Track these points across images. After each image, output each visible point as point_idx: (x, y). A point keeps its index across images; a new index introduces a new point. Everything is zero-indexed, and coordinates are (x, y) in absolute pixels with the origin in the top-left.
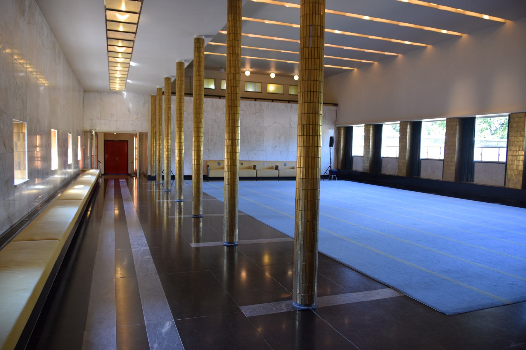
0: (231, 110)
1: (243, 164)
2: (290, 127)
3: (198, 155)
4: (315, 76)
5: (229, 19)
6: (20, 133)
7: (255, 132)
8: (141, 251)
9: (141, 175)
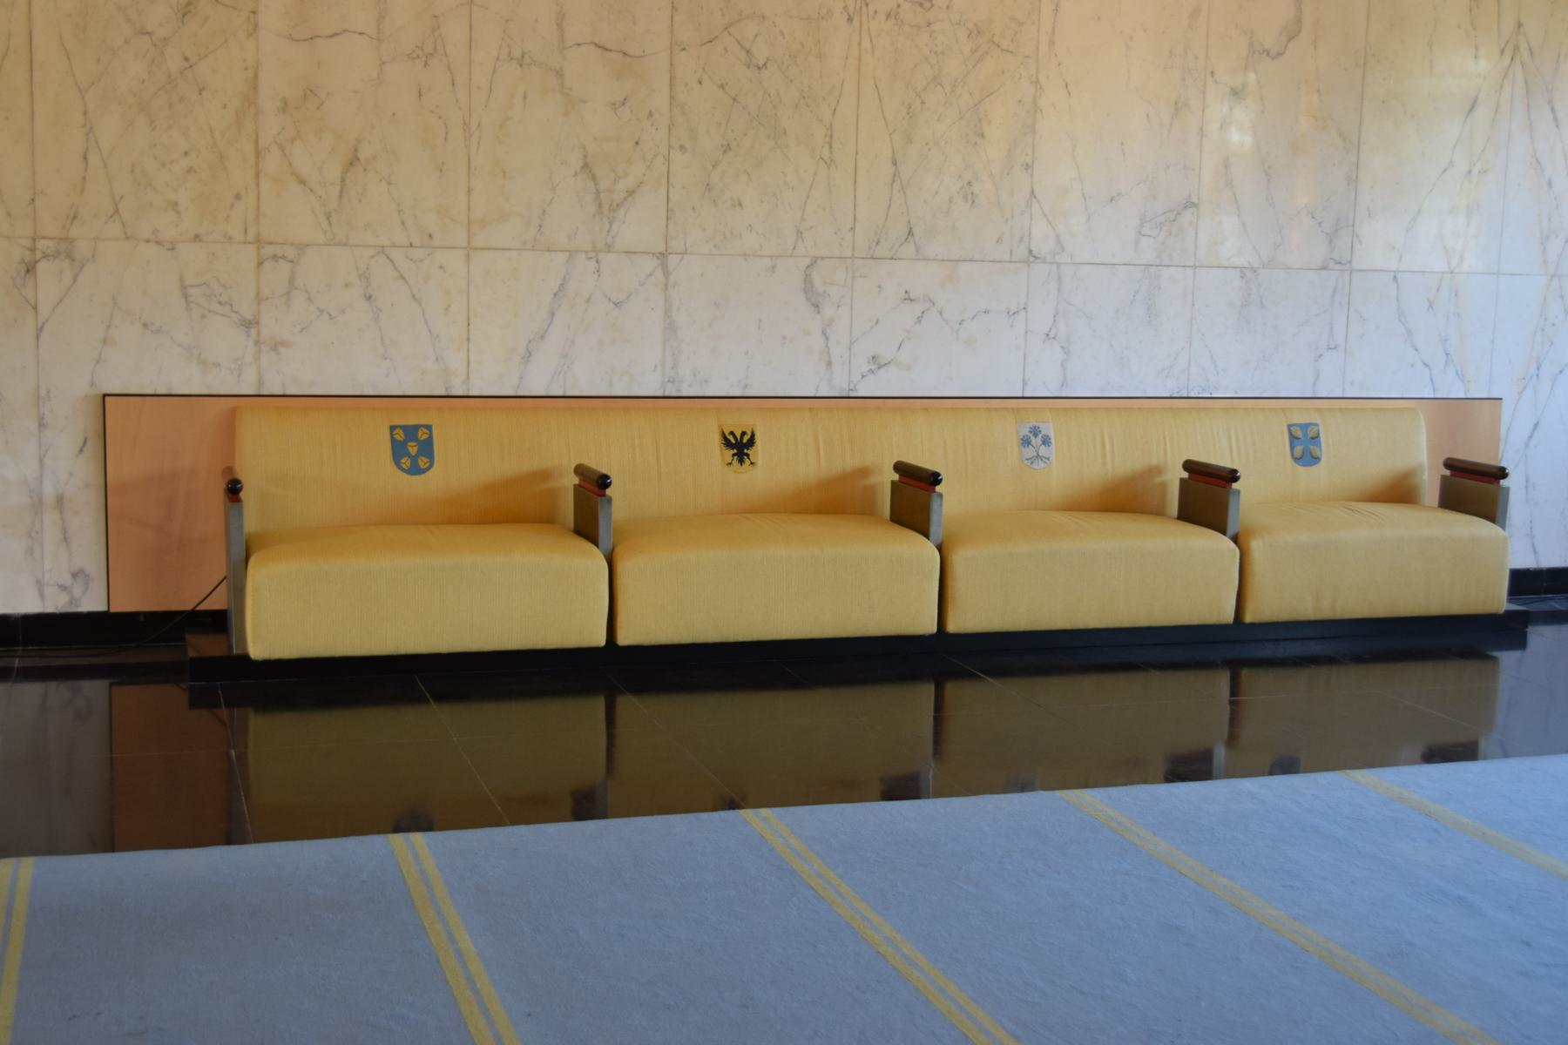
1: (758, 452)
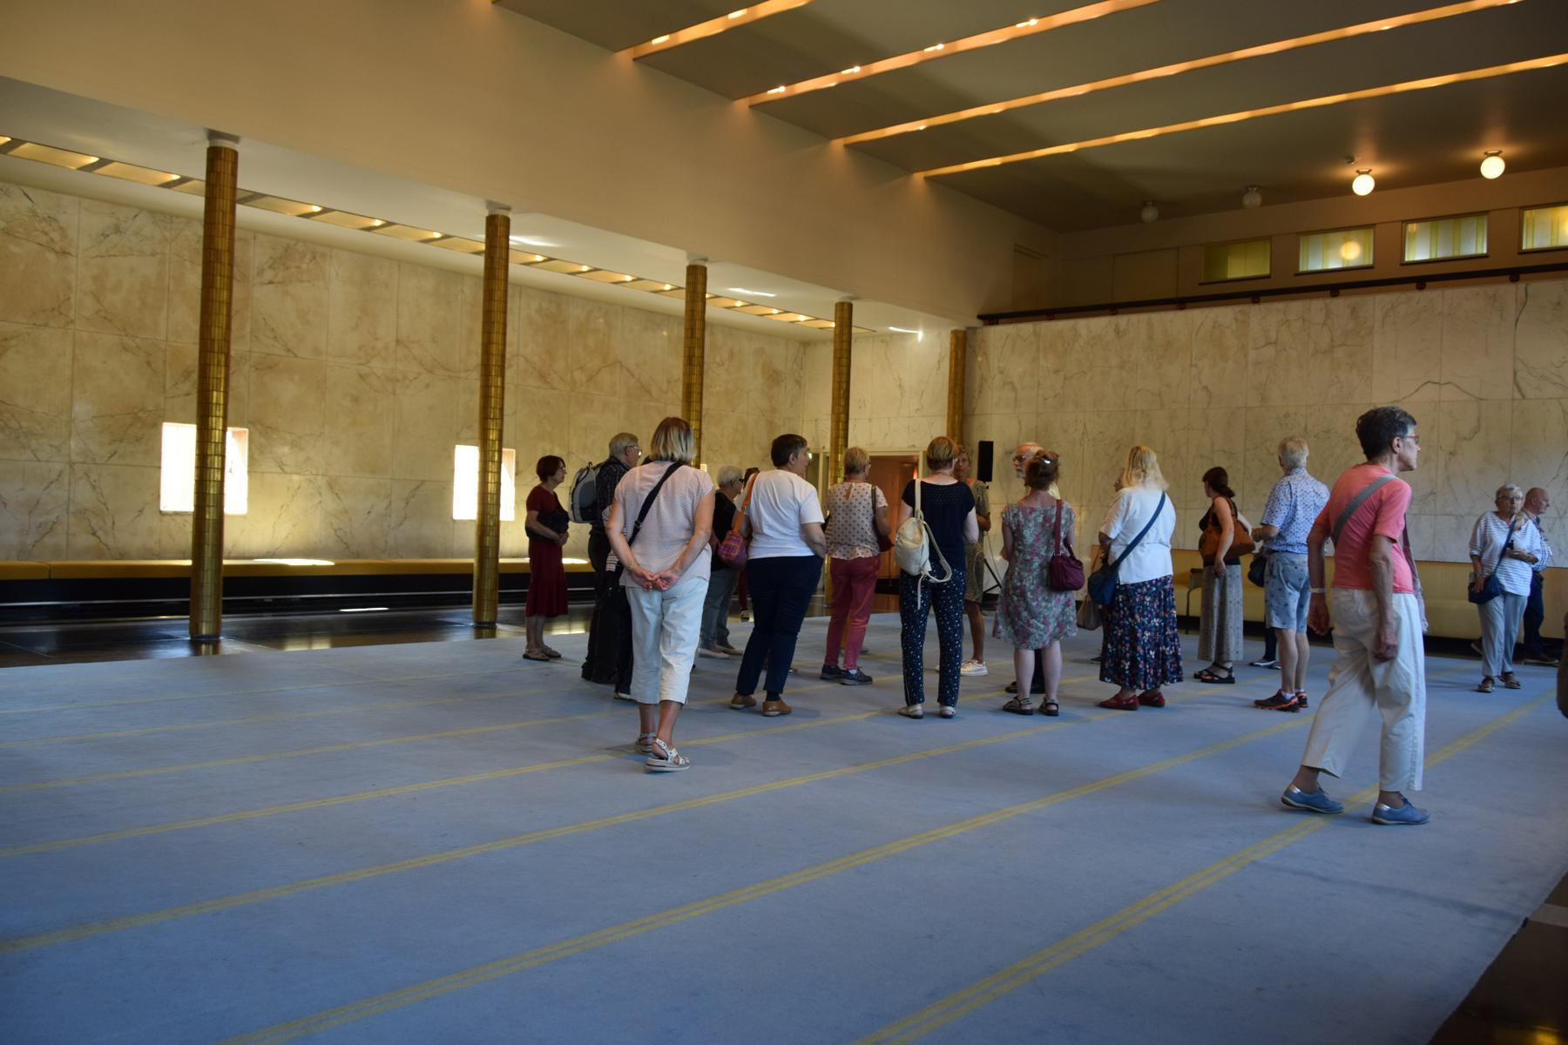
2: (1513, 399)
7: (1328, 431)
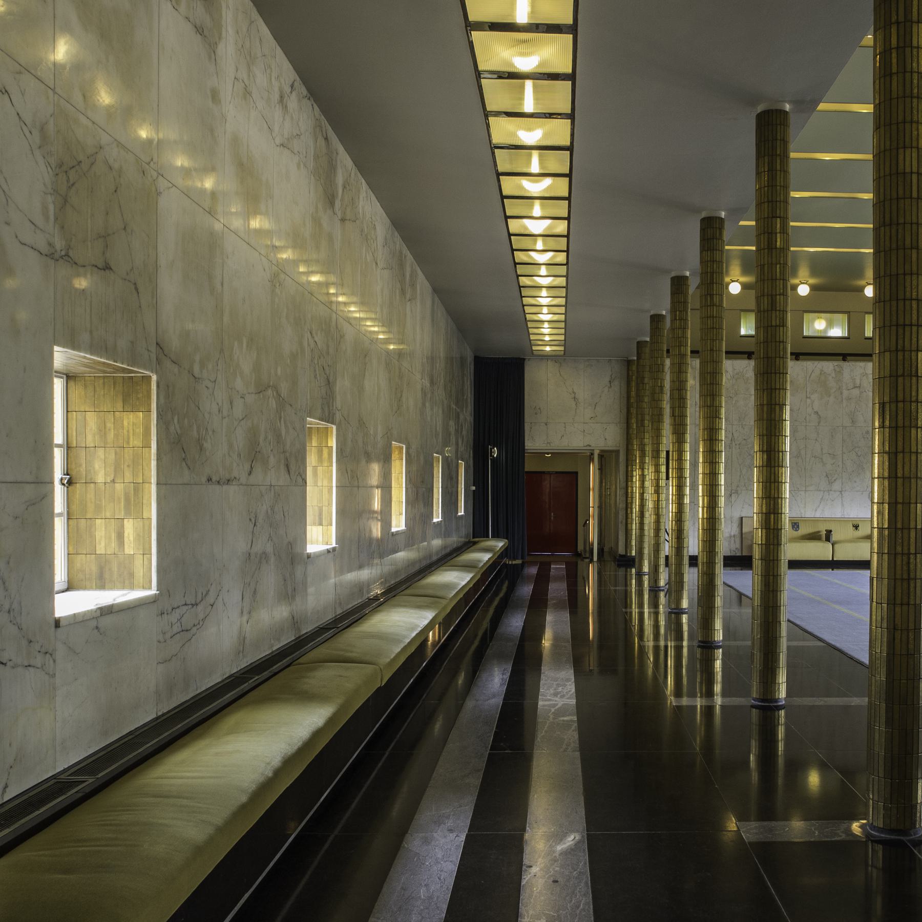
0: (765, 383)
1: (860, 528)
3: (710, 496)
4: (908, 289)
5: (760, 171)
6: (324, 448)
8: (557, 707)
9: (607, 557)
